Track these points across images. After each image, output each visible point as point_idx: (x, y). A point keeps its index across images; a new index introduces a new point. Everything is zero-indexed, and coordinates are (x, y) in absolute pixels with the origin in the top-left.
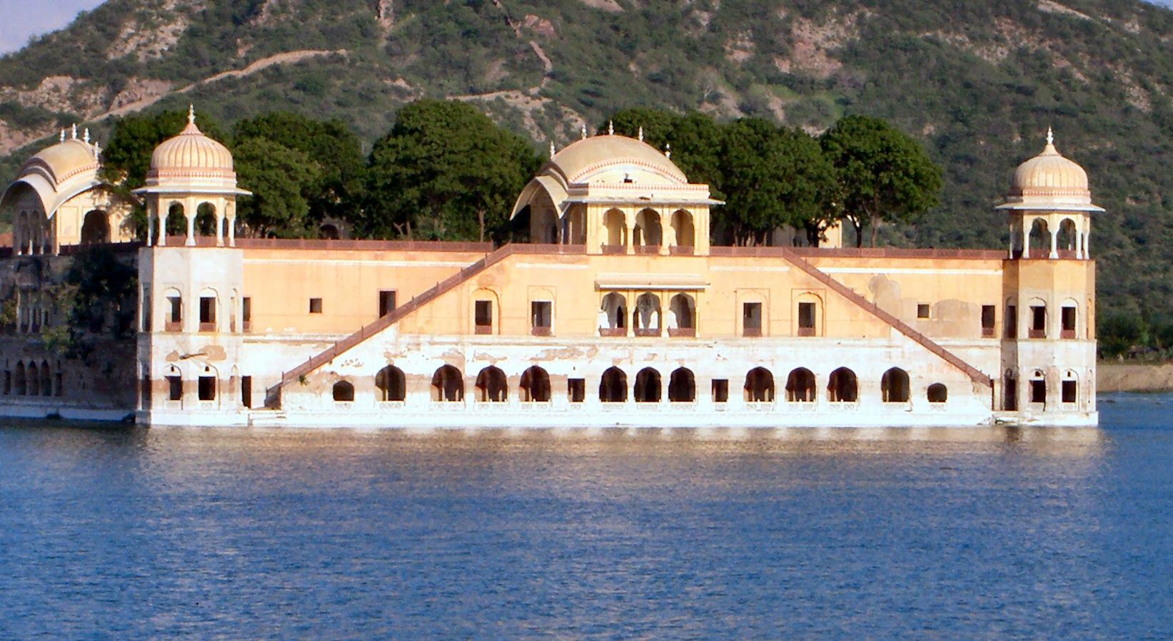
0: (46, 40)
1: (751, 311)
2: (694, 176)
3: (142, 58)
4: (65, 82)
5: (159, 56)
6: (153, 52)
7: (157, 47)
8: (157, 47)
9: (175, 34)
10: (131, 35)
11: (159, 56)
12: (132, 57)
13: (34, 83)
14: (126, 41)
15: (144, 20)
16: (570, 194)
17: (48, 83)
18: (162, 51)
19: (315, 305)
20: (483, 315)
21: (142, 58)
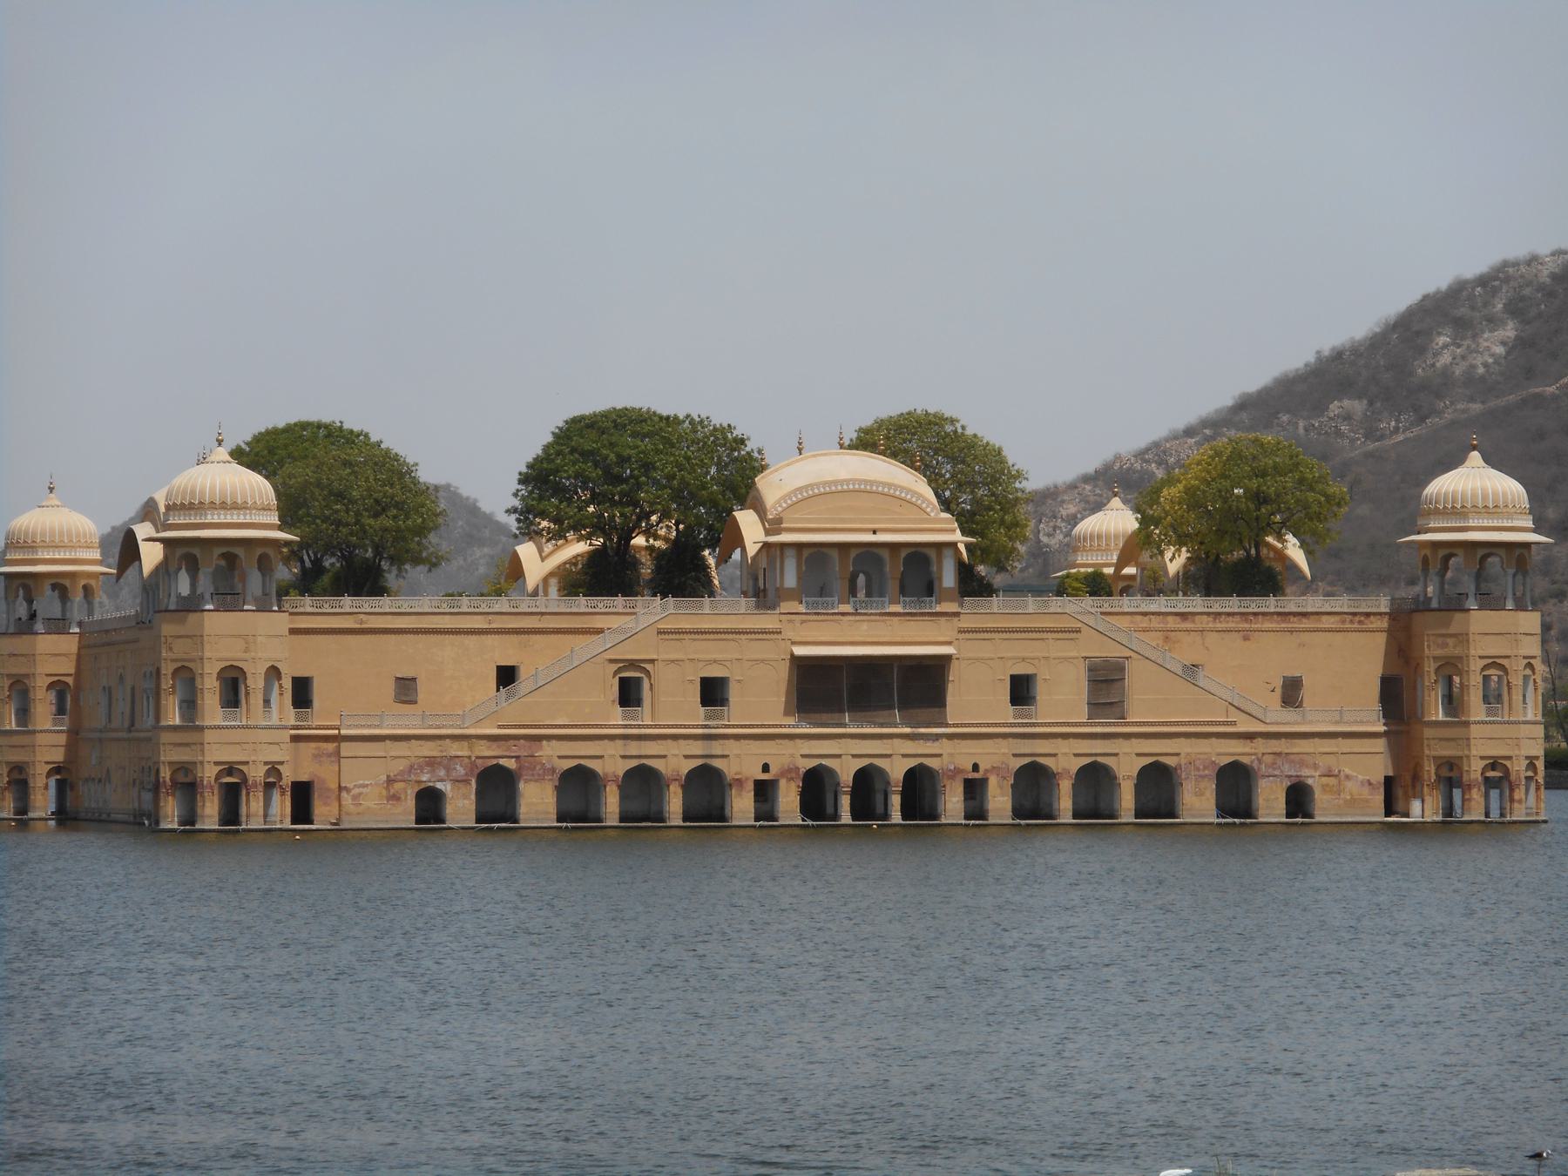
0: (1338, 355)
1: (1021, 690)
2: (946, 505)
3: (1458, 372)
4: (1357, 406)
5: (1481, 370)
6: (1473, 367)
7: (1479, 361)
8: (1479, 361)
9: (1503, 343)
10: (1445, 346)
11: (1481, 370)
12: (1446, 373)
13: (1319, 408)
14: (1436, 354)
15: (1463, 327)
16: (768, 533)
17: (1335, 408)
18: (1486, 365)
19: (406, 689)
20: (629, 694)
21: (1458, 372)
